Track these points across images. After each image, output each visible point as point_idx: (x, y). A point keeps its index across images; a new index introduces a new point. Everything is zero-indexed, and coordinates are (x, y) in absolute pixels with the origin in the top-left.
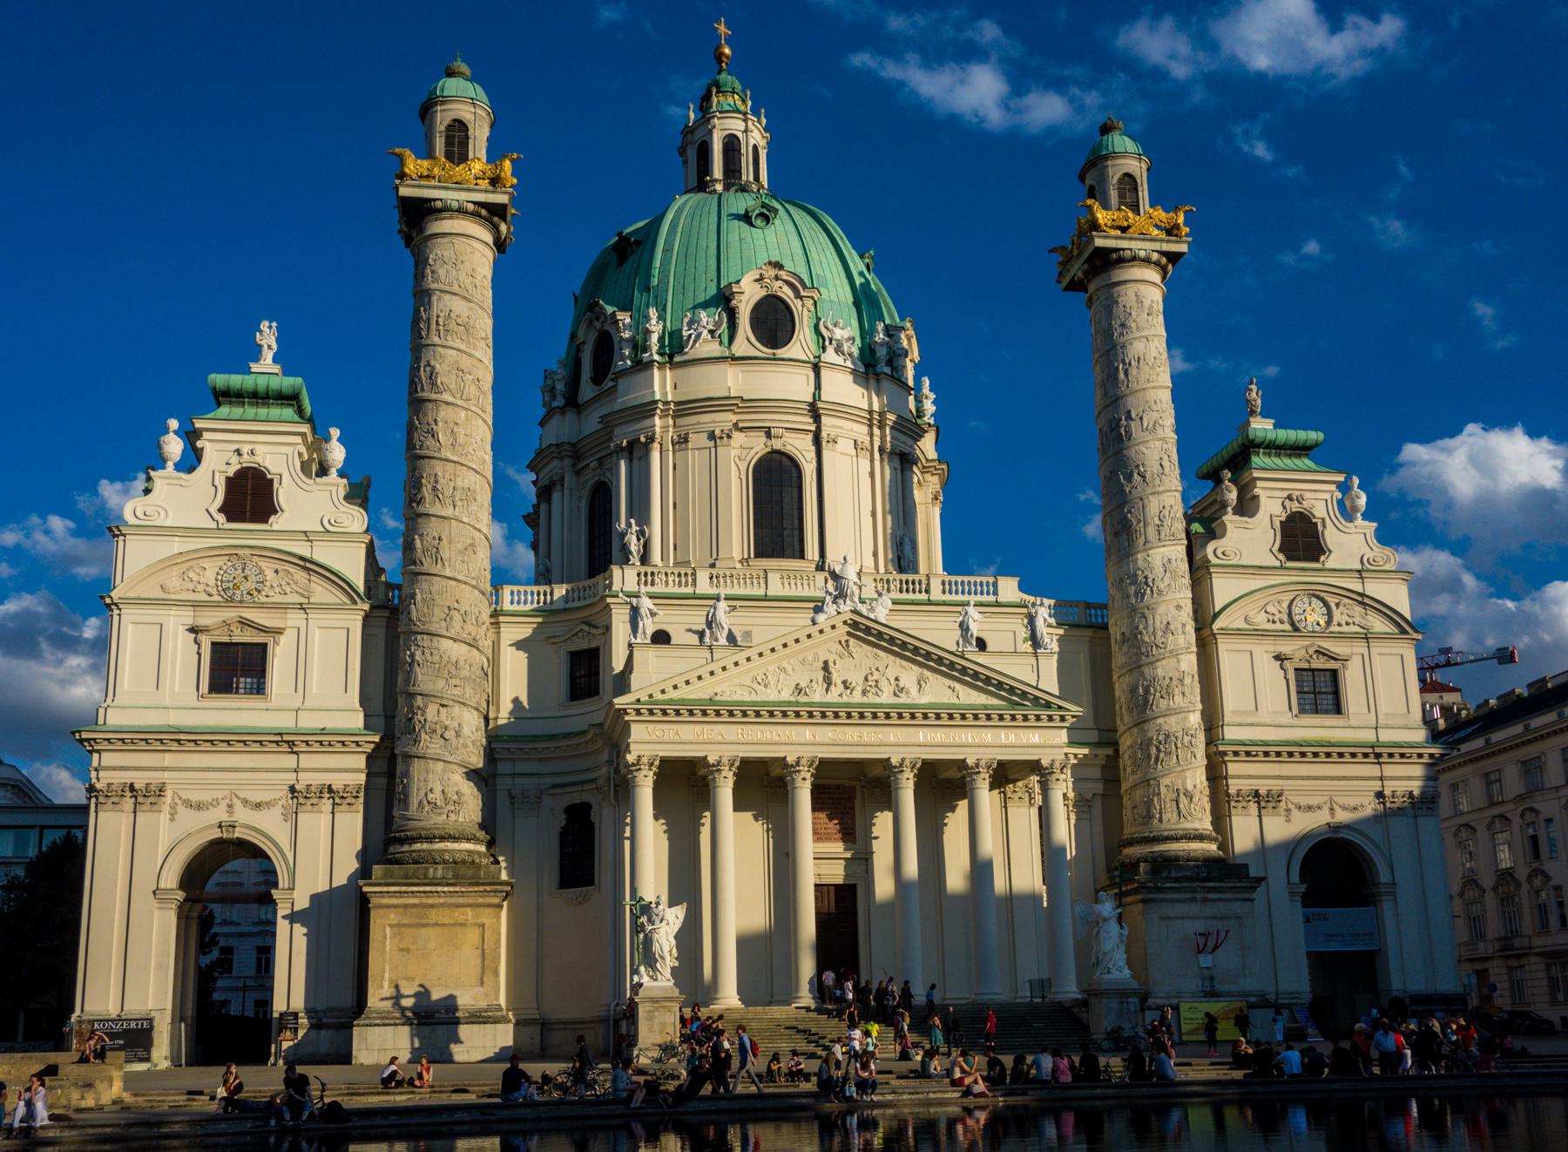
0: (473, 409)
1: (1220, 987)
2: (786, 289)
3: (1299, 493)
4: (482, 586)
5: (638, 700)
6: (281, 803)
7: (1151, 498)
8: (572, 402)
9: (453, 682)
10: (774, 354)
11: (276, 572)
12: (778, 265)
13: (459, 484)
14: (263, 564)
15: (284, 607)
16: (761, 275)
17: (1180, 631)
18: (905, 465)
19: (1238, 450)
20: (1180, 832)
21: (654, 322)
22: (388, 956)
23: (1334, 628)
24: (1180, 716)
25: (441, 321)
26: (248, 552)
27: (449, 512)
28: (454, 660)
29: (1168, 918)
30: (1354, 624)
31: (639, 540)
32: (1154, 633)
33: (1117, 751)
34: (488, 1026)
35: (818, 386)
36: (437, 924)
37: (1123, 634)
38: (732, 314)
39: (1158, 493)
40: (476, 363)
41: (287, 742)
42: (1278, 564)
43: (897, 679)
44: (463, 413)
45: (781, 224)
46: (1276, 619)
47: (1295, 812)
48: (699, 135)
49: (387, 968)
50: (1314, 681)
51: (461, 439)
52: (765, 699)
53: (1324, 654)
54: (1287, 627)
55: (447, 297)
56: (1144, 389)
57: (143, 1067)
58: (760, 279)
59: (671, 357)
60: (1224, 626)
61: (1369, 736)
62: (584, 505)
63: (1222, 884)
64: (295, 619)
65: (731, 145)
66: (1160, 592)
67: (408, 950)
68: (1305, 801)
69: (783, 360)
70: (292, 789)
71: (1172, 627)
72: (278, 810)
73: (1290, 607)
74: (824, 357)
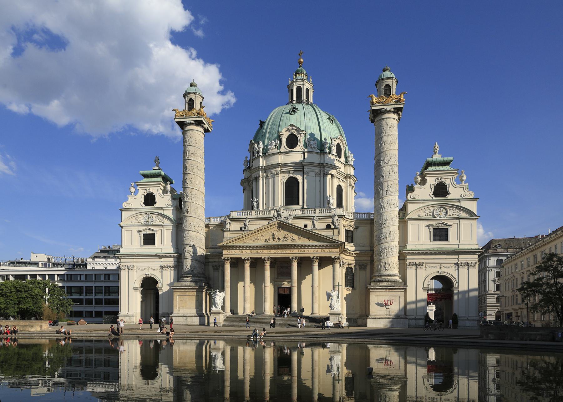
2: (295, 132)
5: (224, 244)
8: (249, 168)
10: (292, 150)
11: (156, 217)
14: (153, 215)
16: (288, 128)
18: (333, 177)
21: (261, 145)
25: (187, 153)
26: (149, 213)
43: (293, 237)
45: (299, 113)
55: (189, 147)
58: (288, 130)
68: (432, 265)
69: (294, 152)
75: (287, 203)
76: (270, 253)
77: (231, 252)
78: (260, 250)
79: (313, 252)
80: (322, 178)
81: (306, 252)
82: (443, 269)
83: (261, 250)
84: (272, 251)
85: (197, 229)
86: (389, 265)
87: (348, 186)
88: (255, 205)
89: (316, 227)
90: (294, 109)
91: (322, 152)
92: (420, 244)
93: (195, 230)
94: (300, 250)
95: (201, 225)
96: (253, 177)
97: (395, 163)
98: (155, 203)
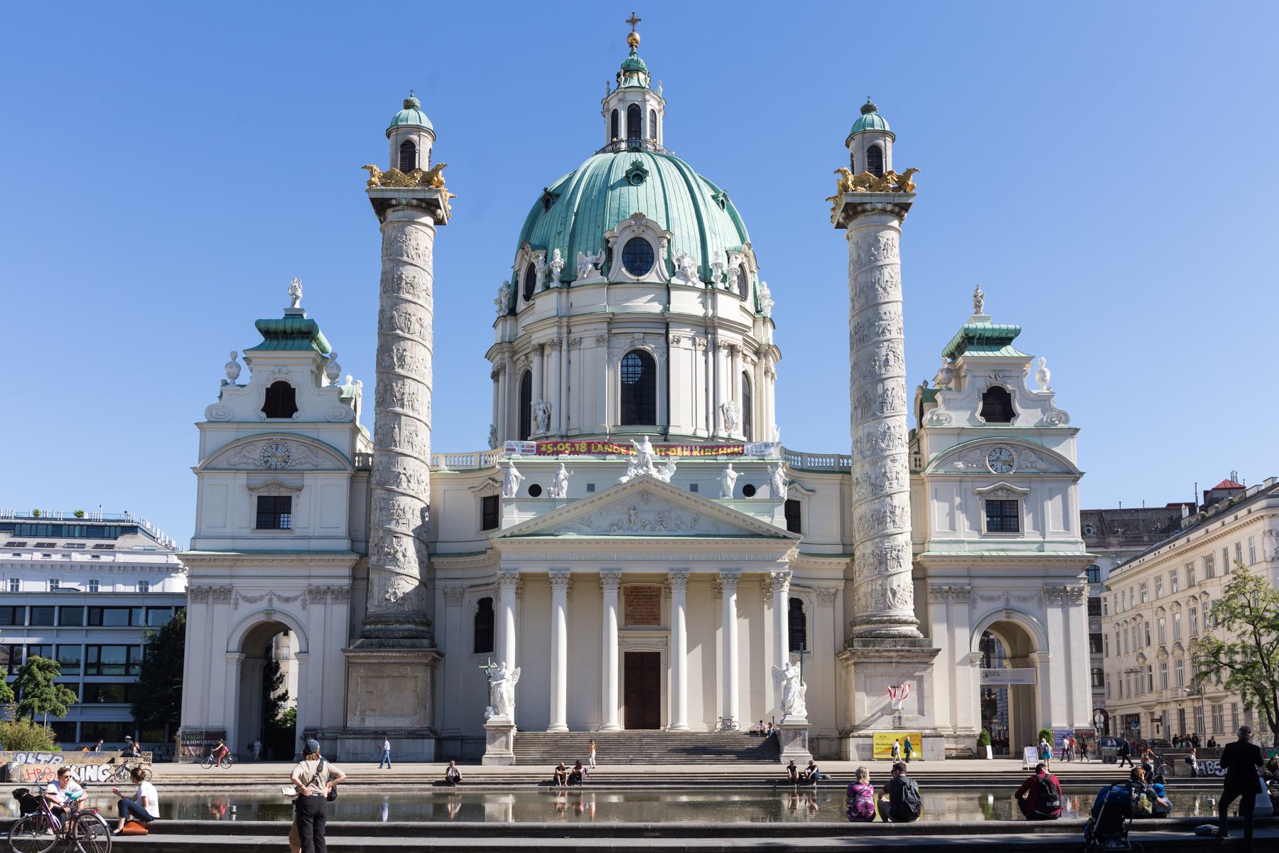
4: (422, 457)
5: (505, 536)
6: (302, 597)
8: (512, 312)
13: (407, 391)
17: (894, 477)
19: (960, 340)
20: (885, 618)
21: (558, 260)
27: (398, 409)
28: (402, 507)
31: (544, 411)
33: (853, 560)
34: (419, 740)
35: (669, 303)
37: (857, 479)
38: (610, 252)
45: (652, 180)
48: (613, 104)
50: (1001, 509)
59: (569, 283)
62: (518, 384)
64: (309, 479)
65: (635, 114)
68: (988, 594)
69: (644, 283)
71: (889, 475)
72: (299, 603)
74: (672, 282)
75: (626, 420)
80: (710, 354)
82: (1014, 604)
88: (539, 418)
90: (639, 172)
91: (710, 287)
96: (533, 342)
97: (899, 336)
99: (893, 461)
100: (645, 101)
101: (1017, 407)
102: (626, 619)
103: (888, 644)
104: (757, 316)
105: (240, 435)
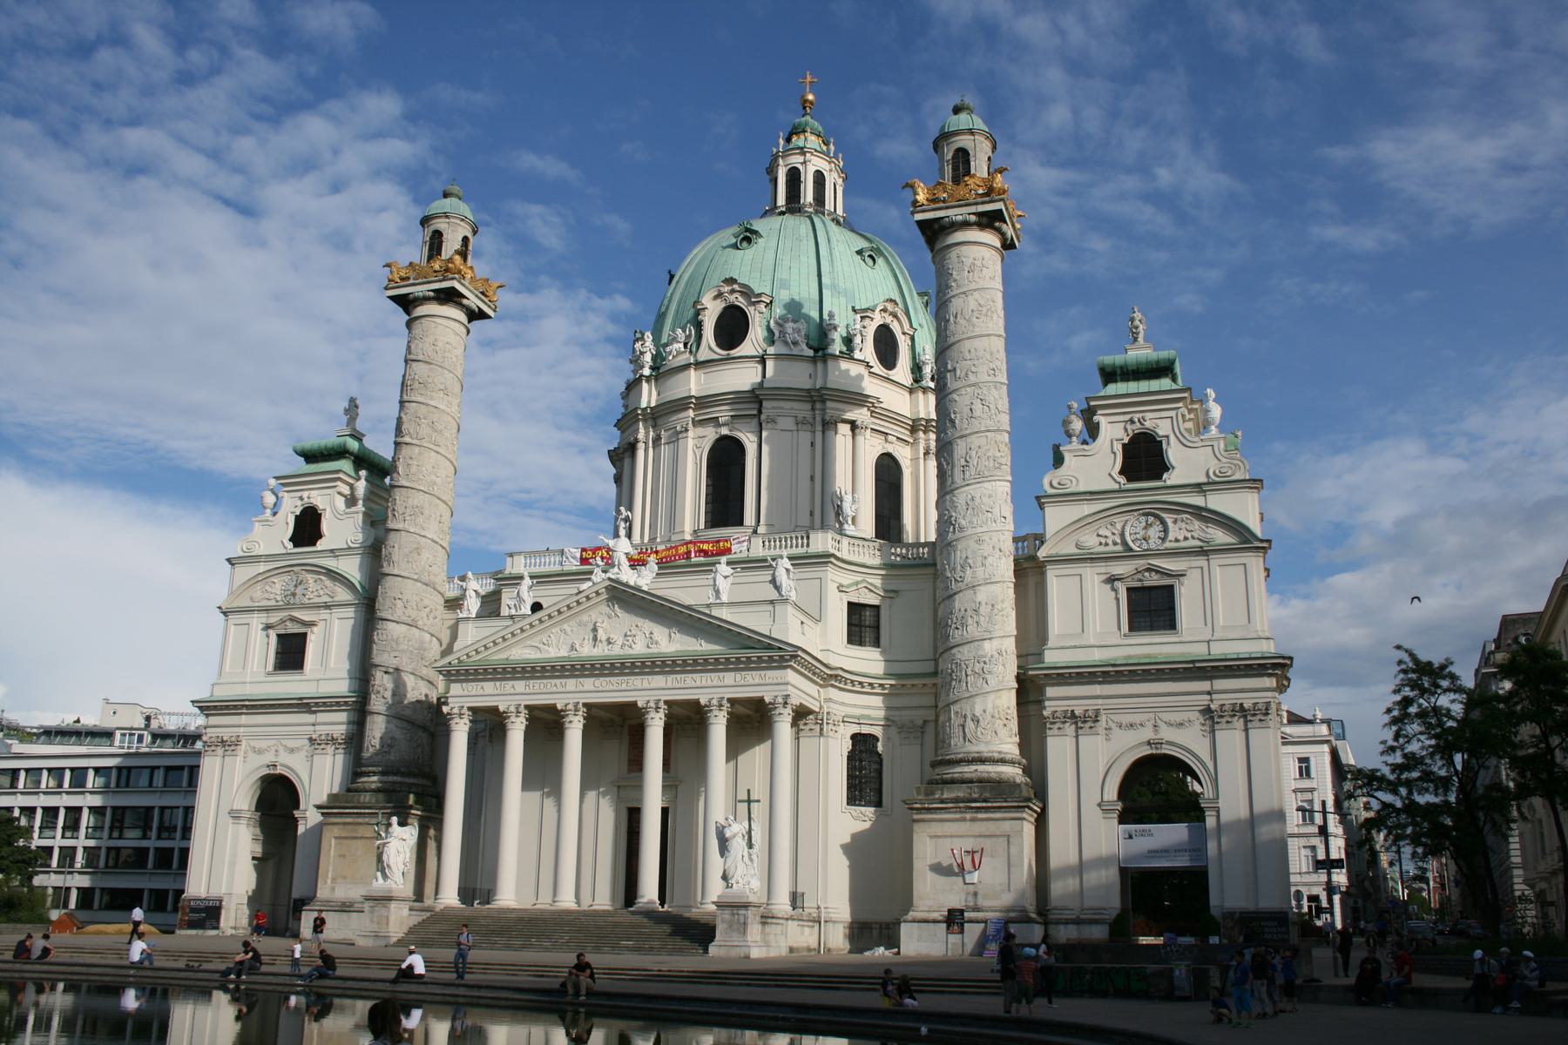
0: (425, 445)
1: (982, 902)
2: (740, 299)
3: (1140, 415)
4: (425, 578)
5: (450, 663)
7: (959, 441)
9: (393, 654)
11: (316, 581)
12: (731, 281)
14: (309, 576)
15: (318, 607)
17: (979, 564)
18: (857, 431)
20: (960, 756)
22: (331, 860)
23: (1168, 545)
24: (972, 645)
27: (399, 526)
28: (395, 637)
29: (939, 837)
30: (1193, 537)
32: (954, 569)
36: (362, 838)
38: (699, 326)
39: (965, 436)
40: (431, 409)
41: (304, 705)
42: (1116, 487)
43: (651, 633)
44: (417, 450)
46: (1110, 542)
47: (1116, 731)
49: (331, 868)
51: (414, 469)
52: (547, 656)
53: (1157, 572)
54: (1119, 548)
56: (959, 341)
57: (213, 932)
58: (719, 295)
59: (658, 368)
60: (1053, 552)
61: (1199, 651)
63: (989, 804)
64: (324, 614)
65: (794, 177)
66: (961, 529)
67: (343, 856)
68: (1127, 719)
70: (311, 740)
71: (969, 561)
72: (303, 754)
73: (1123, 528)
76: (581, 688)
77: (473, 688)
78: (553, 681)
79: (709, 683)
80: (819, 435)
81: (690, 685)
82: (1167, 734)
83: (558, 681)
84: (588, 683)
85: (413, 616)
86: (978, 722)
87: (922, 455)
89: (725, 598)
91: (820, 354)
92: (1087, 643)
93: (405, 619)
94: (671, 678)
95: (426, 602)
98: (320, 536)
99: (979, 541)
100: (804, 163)
101: (1173, 453)
102: (629, 765)
103: (960, 792)
104: (916, 385)
105: (262, 568)
